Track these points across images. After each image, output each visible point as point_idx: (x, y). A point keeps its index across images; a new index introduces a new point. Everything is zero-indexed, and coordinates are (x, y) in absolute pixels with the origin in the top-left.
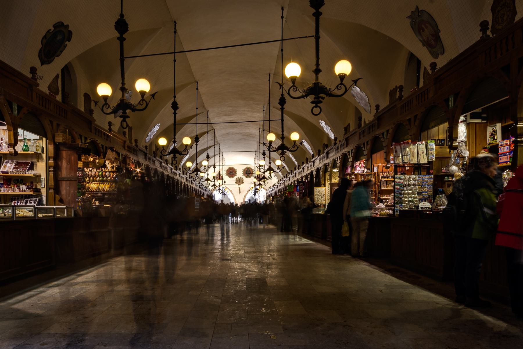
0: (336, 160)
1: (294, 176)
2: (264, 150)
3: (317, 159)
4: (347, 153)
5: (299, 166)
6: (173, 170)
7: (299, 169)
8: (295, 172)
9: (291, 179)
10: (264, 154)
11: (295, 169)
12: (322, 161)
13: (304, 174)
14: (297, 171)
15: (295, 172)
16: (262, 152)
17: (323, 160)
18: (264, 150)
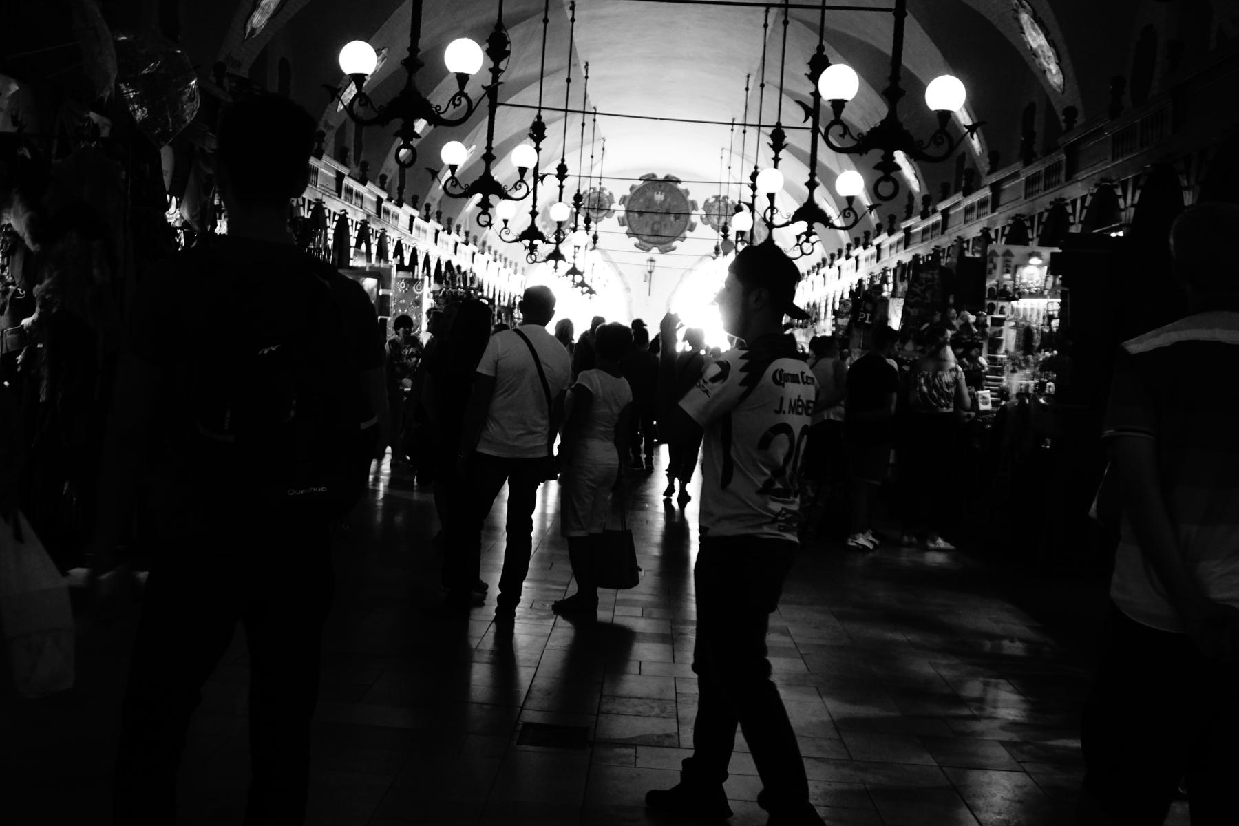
0: (1028, 224)
1: (898, 242)
2: (779, 125)
3: (958, 204)
4: (1026, 220)
5: (927, 200)
6: (349, 182)
7: (925, 216)
8: (904, 225)
9: (885, 256)
10: (778, 140)
11: (908, 217)
12: (974, 215)
13: (945, 241)
14: (916, 224)
15: (904, 225)
16: (770, 131)
17: (982, 211)
18: (779, 125)
